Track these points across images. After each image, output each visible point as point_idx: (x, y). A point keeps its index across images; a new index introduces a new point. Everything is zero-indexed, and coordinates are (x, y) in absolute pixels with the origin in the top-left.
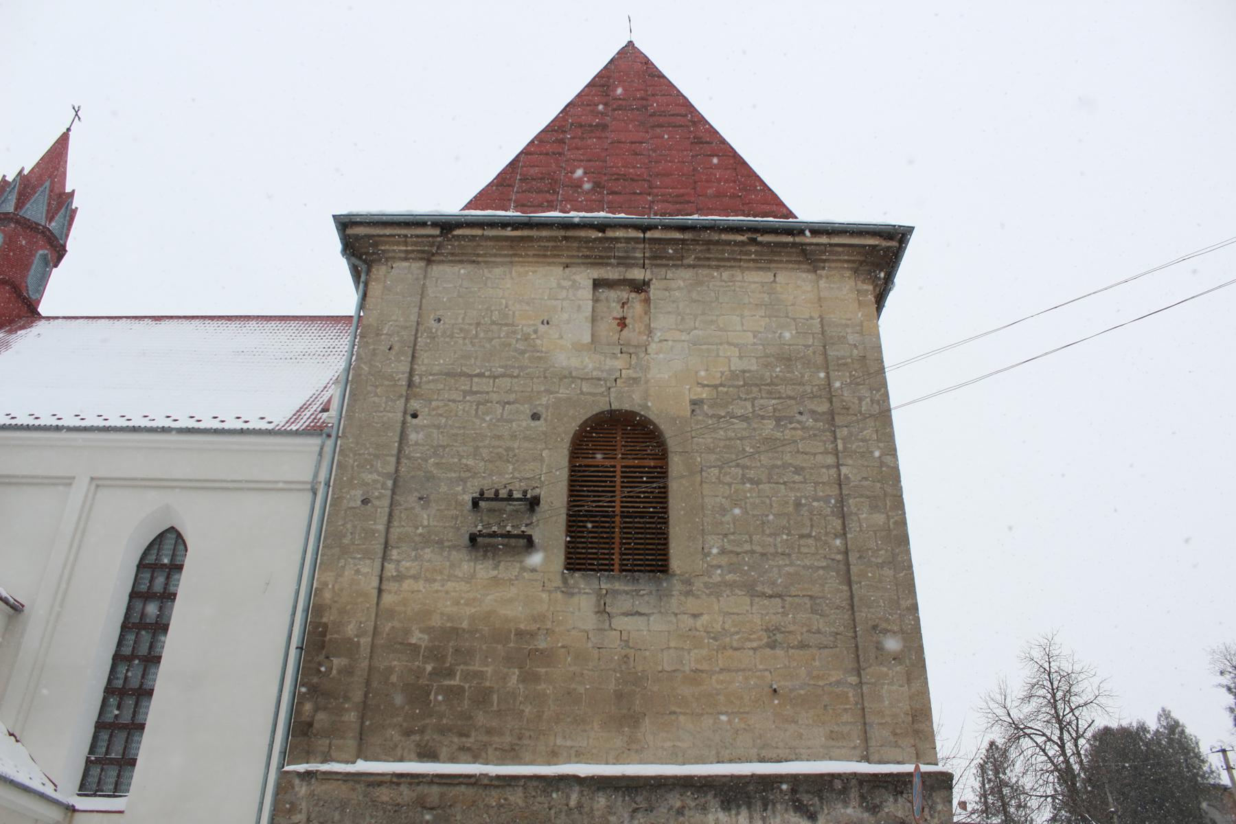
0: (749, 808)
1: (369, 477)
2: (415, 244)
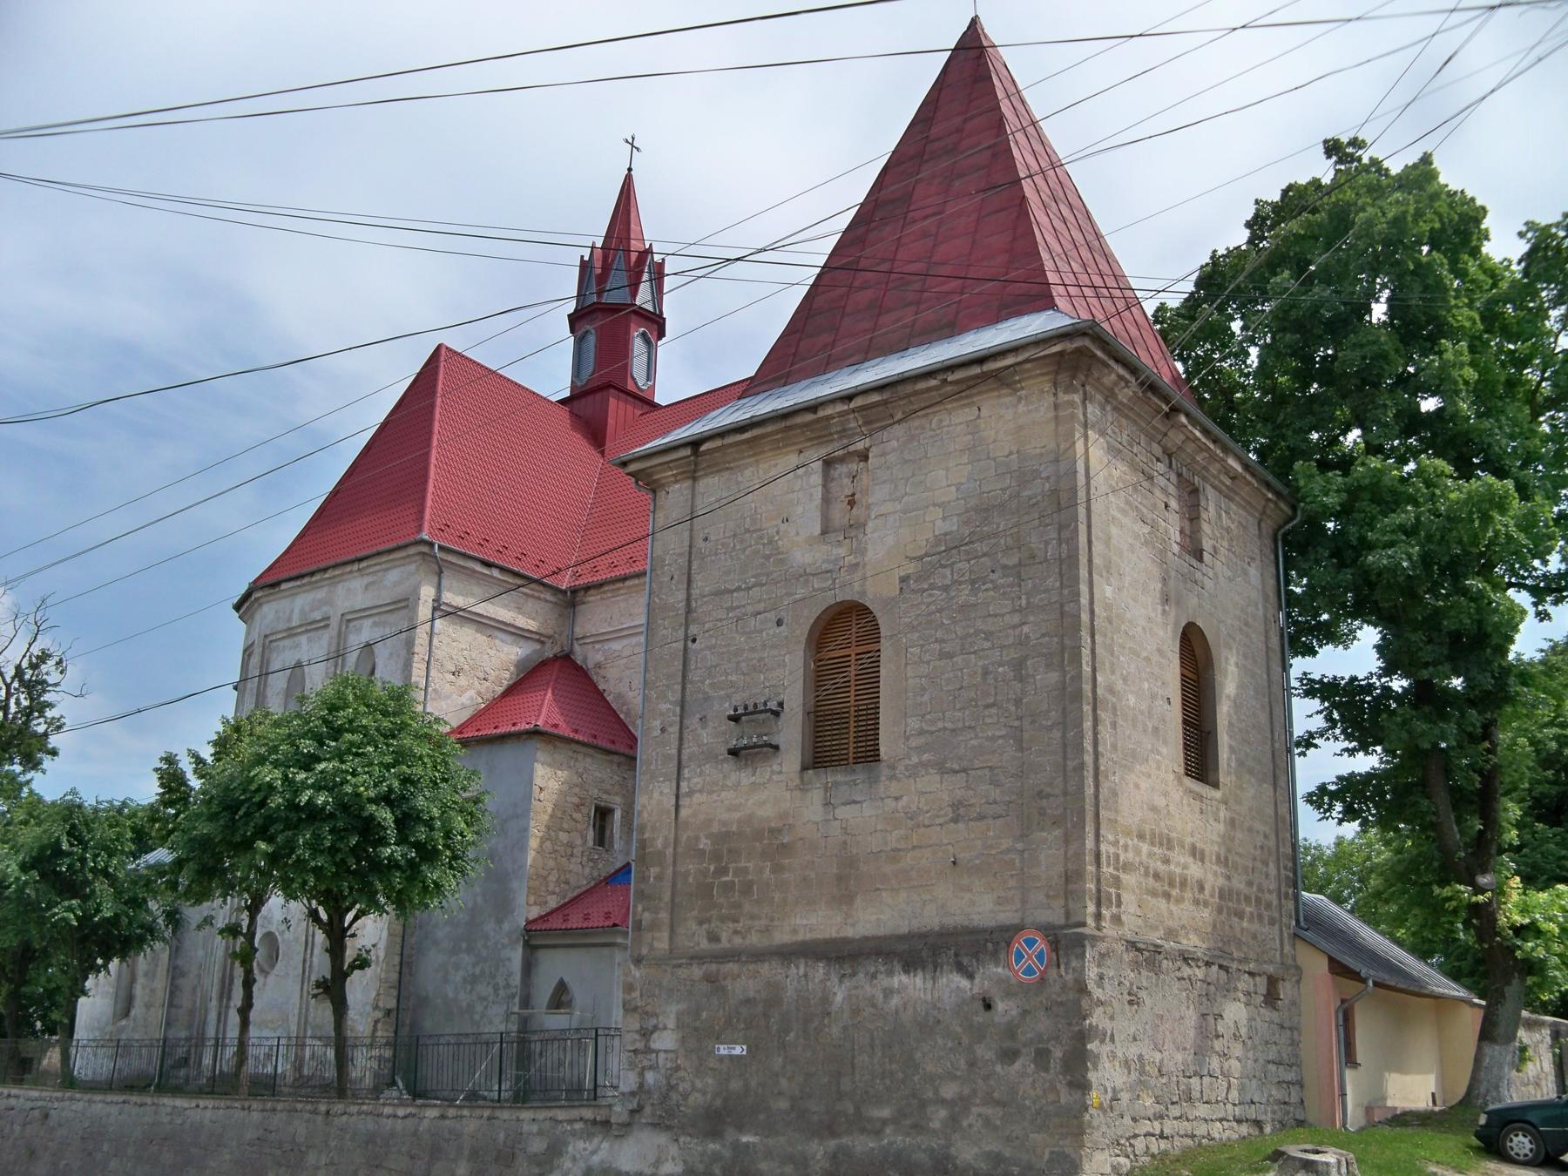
1: (664, 707)
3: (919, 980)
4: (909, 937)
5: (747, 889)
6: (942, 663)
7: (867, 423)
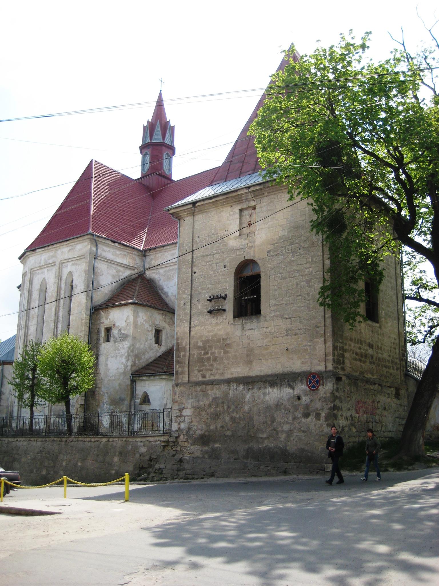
1: (185, 296)
5: (215, 360)
6: (282, 281)
7: (254, 196)
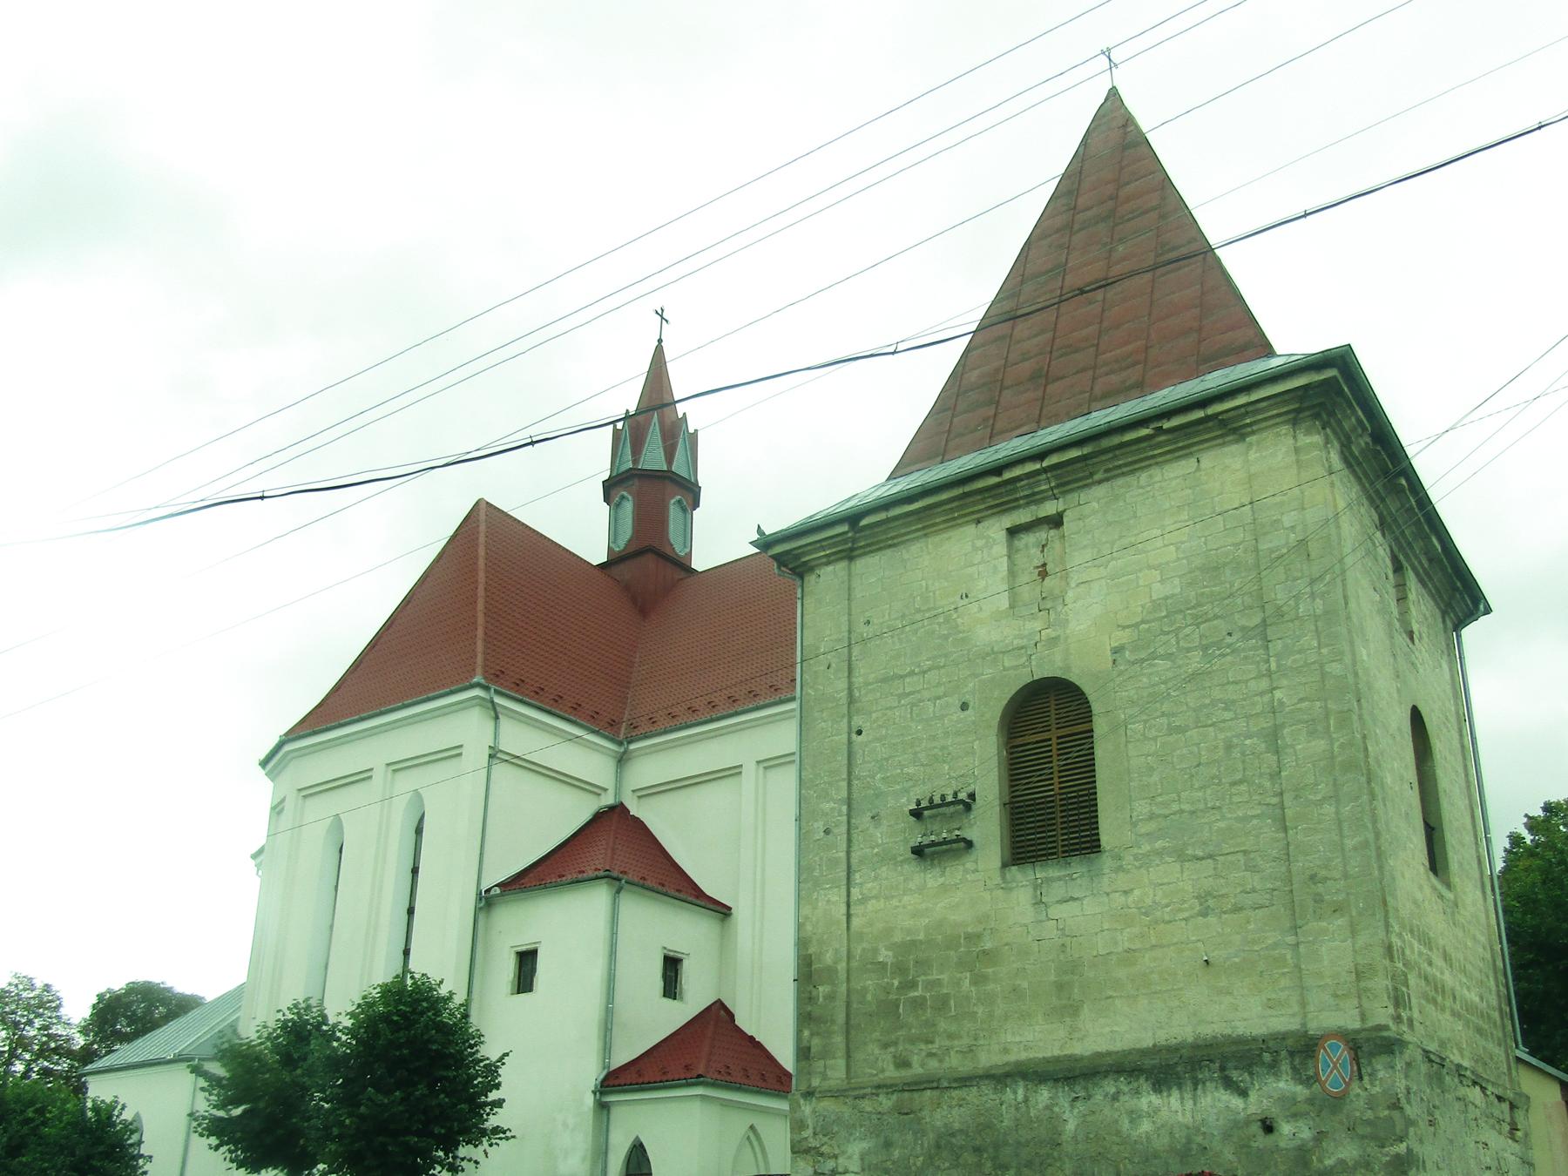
0: (1180, 1088)
1: (827, 806)
2: (830, 546)
3: (1174, 1099)
4: (1156, 1050)
6: (1170, 739)
